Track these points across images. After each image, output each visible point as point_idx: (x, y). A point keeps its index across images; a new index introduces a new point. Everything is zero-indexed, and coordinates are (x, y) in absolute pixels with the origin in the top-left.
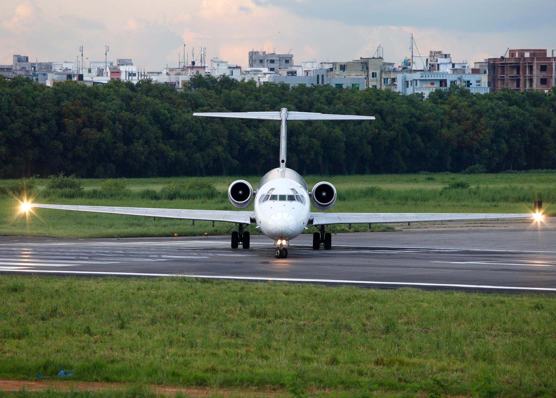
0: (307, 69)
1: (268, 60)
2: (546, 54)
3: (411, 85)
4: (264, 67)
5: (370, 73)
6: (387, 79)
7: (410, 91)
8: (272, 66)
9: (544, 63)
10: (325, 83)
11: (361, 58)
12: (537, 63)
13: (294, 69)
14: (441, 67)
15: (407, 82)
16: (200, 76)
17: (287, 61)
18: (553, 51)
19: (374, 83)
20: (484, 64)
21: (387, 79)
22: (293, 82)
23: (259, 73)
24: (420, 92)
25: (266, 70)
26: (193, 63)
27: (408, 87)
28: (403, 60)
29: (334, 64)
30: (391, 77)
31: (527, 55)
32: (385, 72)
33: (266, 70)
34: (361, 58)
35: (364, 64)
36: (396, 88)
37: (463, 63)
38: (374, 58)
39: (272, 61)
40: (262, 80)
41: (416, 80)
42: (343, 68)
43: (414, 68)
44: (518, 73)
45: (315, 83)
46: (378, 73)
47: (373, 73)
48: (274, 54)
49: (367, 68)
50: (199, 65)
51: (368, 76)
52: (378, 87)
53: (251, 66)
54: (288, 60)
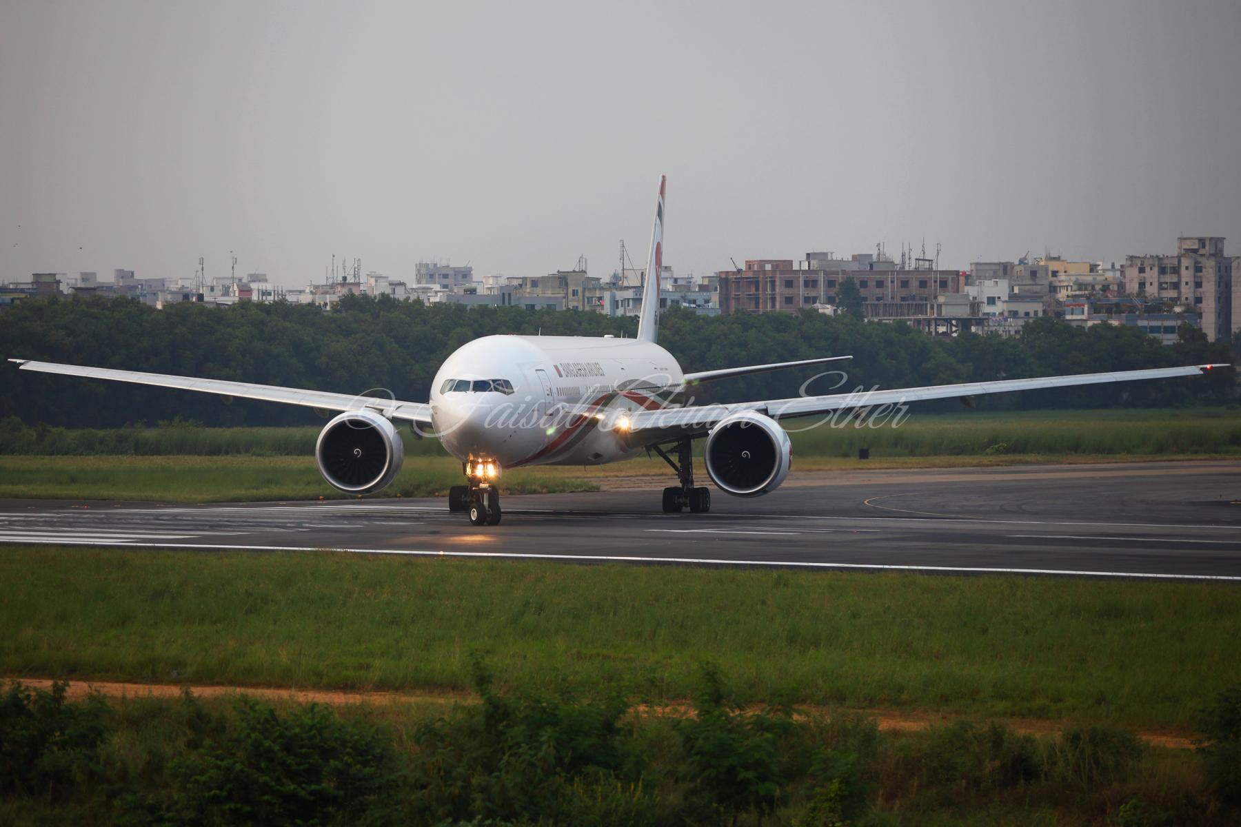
0: (490, 286)
1: (440, 275)
3: (622, 306)
4: (435, 283)
5: (570, 290)
6: (592, 298)
7: (620, 312)
8: (445, 281)
9: (789, 277)
10: (513, 304)
11: (558, 272)
13: (474, 285)
16: (353, 295)
17: (465, 276)
18: (800, 262)
19: (575, 304)
21: (592, 298)
22: (471, 303)
23: (429, 290)
25: (437, 287)
26: (345, 279)
28: (612, 274)
29: (524, 279)
30: (597, 296)
31: (768, 267)
32: (590, 290)
33: (437, 287)
34: (558, 272)
35: (562, 279)
38: (574, 271)
39: (446, 276)
40: (433, 300)
41: (628, 299)
42: (535, 283)
43: (626, 284)
44: (757, 289)
45: (501, 305)
46: (580, 290)
47: (574, 290)
48: (448, 266)
49: (567, 284)
50: (352, 281)
51: (567, 294)
52: (580, 309)
53: (419, 282)
54: (465, 274)
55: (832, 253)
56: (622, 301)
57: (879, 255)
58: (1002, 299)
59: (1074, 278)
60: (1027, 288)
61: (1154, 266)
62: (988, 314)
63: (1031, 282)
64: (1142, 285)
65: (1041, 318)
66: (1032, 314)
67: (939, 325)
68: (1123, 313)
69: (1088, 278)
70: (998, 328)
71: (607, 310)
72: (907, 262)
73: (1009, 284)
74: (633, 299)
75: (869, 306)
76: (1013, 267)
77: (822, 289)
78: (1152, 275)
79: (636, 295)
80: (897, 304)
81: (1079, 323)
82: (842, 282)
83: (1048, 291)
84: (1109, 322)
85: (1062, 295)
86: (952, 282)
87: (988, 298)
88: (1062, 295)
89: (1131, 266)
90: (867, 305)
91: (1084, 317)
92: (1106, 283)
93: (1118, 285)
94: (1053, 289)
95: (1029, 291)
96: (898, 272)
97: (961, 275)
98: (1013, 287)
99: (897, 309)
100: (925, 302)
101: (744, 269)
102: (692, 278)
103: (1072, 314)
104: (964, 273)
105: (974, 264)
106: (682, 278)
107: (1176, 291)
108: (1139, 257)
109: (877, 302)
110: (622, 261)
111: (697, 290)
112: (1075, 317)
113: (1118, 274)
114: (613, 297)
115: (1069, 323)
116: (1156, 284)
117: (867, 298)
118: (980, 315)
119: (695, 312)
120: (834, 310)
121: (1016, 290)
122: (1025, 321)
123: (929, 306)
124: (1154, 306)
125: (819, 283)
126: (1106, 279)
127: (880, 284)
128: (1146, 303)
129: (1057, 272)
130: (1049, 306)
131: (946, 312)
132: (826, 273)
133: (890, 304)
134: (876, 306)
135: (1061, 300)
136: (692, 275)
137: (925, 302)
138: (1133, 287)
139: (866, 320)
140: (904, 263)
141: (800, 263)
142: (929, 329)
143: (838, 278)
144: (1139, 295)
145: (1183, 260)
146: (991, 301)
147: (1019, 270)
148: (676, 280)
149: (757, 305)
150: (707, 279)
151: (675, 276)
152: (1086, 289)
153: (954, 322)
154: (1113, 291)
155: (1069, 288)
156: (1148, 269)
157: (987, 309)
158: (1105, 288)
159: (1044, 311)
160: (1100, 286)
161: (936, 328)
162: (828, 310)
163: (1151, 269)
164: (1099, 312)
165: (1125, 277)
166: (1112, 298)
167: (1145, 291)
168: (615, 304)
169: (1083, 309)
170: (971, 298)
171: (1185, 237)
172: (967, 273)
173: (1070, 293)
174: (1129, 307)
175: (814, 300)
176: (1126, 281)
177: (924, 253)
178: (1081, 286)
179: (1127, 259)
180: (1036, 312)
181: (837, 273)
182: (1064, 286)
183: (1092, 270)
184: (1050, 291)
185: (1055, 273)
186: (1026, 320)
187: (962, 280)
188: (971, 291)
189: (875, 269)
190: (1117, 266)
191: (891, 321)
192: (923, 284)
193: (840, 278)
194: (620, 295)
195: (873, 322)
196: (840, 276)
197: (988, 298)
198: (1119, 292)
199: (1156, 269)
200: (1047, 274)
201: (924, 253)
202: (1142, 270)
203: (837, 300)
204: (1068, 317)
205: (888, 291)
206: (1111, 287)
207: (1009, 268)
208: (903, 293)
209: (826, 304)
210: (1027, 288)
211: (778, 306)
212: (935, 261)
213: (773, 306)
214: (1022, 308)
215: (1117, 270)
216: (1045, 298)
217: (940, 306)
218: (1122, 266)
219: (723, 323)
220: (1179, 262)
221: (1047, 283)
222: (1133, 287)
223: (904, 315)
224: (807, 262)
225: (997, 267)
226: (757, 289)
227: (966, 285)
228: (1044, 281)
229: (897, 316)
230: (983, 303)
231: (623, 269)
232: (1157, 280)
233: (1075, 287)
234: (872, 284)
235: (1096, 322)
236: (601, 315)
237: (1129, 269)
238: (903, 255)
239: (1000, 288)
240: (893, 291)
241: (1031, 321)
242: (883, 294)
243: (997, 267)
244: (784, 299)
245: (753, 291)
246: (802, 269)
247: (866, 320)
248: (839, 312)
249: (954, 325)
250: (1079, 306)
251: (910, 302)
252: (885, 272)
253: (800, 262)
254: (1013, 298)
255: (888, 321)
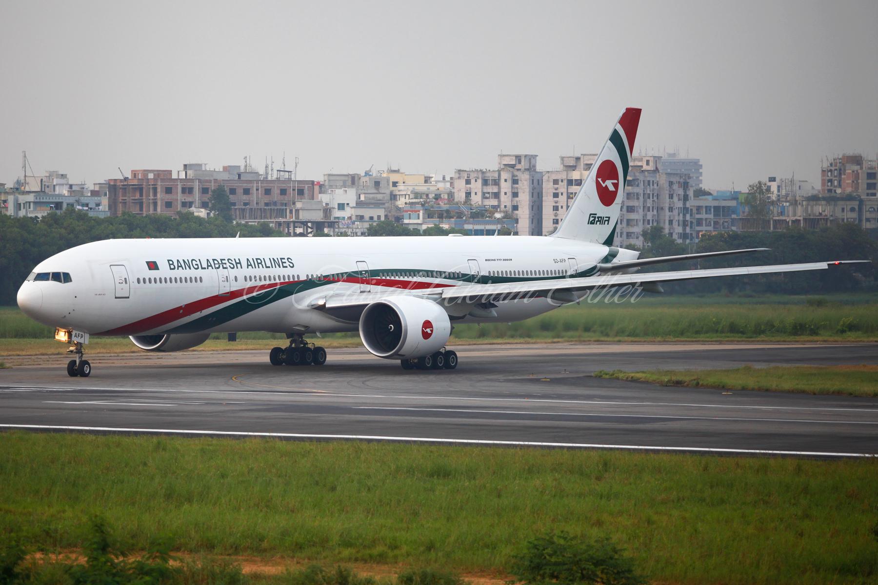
2: (171, 174)
3: (24, 208)
7: (22, 213)
9: (168, 185)
12: (161, 185)
14: (57, 188)
15: (20, 204)
18: (179, 172)
20: (103, 185)
24: (33, 215)
27: (20, 210)
30: (2, 199)
31: (151, 176)
36: (7, 210)
37: (82, 185)
41: (30, 202)
43: (27, 189)
44: (141, 195)
55: (205, 165)
56: (24, 204)
57: (246, 166)
58: (351, 205)
59: (411, 188)
60: (371, 196)
61: (478, 178)
62: (338, 218)
63: (375, 191)
64: (468, 194)
65: (383, 222)
66: (375, 219)
67: (297, 227)
68: (453, 218)
69: (423, 188)
70: (347, 230)
71: (10, 211)
72: (270, 172)
73: (357, 192)
74: (34, 203)
75: (237, 211)
76: (360, 178)
77: (197, 195)
78: (476, 186)
79: (36, 198)
80: (261, 209)
81: (416, 227)
82: (214, 190)
83: (389, 198)
84: (441, 226)
85: (401, 202)
86: (308, 190)
87: (339, 204)
88: (401, 202)
89: (459, 178)
90: (236, 209)
91: (419, 221)
92: (438, 192)
93: (448, 194)
94: (394, 197)
95: (373, 198)
96: (262, 181)
97: (316, 185)
98: (360, 195)
99: (261, 214)
100: (284, 207)
101: (130, 177)
102: (85, 184)
103: (410, 218)
104: (318, 183)
105: (327, 175)
106: (76, 185)
107: (497, 200)
108: (465, 171)
109: (244, 207)
110: (24, 169)
111: (89, 194)
112: (412, 221)
113: (448, 185)
114: (16, 200)
115: (406, 226)
116: (480, 194)
117: (235, 203)
118: (332, 219)
119: (88, 214)
120: (208, 213)
121: (362, 198)
122: (370, 225)
123: (288, 211)
124: (479, 213)
125: (194, 190)
126: (438, 189)
127: (247, 192)
128: (471, 209)
129: (397, 182)
130: (390, 212)
131: (303, 216)
132: (200, 181)
133: (255, 209)
134: (243, 210)
135: (400, 206)
136: (85, 182)
137: (284, 207)
138: (460, 196)
139: (235, 222)
140: (267, 174)
141: (178, 173)
142: (288, 230)
143: (211, 185)
144: (465, 203)
145: (502, 173)
146: (341, 207)
147: (364, 181)
148: (71, 186)
149: (141, 209)
150: (98, 186)
151: (70, 183)
152: (421, 198)
153: (309, 225)
154: (444, 199)
155: (407, 196)
156: (473, 181)
157: (337, 213)
158: (437, 197)
159: (386, 216)
160: (433, 195)
161: (294, 230)
162: (202, 213)
163: (476, 181)
164: (432, 218)
165: (453, 188)
166: (444, 206)
167: (470, 200)
168: (18, 206)
169: (419, 215)
170: (324, 205)
171: (504, 153)
172: (321, 183)
173: (408, 201)
174: (458, 213)
175: (190, 204)
176: (455, 191)
177: (284, 165)
178: (417, 195)
179: (455, 172)
180: (379, 217)
181: (210, 181)
182: (403, 195)
183: (426, 182)
184: (391, 199)
185: (395, 184)
186: (371, 223)
187: (317, 188)
188: (324, 198)
189: (242, 178)
190: (448, 179)
191: (256, 224)
192: (283, 192)
193: (213, 186)
194: (22, 199)
195: (241, 223)
196: (213, 184)
197: (339, 204)
198: (449, 200)
199: (480, 181)
200: (388, 185)
201: (284, 165)
202: (468, 182)
203: (210, 205)
204: (406, 221)
205: (254, 197)
206: (442, 196)
207: (356, 179)
208: (266, 199)
209: (201, 208)
210: (371, 196)
211: (159, 210)
212: (293, 173)
213: (155, 209)
214: (367, 213)
215: (448, 181)
216: (386, 205)
217: (297, 211)
218: (451, 178)
219: (112, 224)
220: (499, 175)
221: (388, 192)
222: (460, 196)
223: (268, 219)
224: (184, 172)
225: (346, 178)
226: (141, 195)
227: (320, 193)
228: (386, 190)
229: (261, 219)
230: (334, 208)
231: (25, 176)
232: (481, 191)
233: (412, 196)
234: (240, 191)
235: (430, 226)
236: (6, 215)
237: (458, 180)
238: (266, 167)
239: (349, 196)
240: (258, 197)
241: (375, 224)
242: (249, 200)
243: (346, 178)
244: (164, 203)
245: (137, 196)
246: (180, 178)
247: (235, 222)
248: (212, 215)
249: (310, 228)
250: (416, 211)
251: (273, 207)
252: (250, 182)
253: (179, 172)
254: (360, 204)
255: (253, 223)
